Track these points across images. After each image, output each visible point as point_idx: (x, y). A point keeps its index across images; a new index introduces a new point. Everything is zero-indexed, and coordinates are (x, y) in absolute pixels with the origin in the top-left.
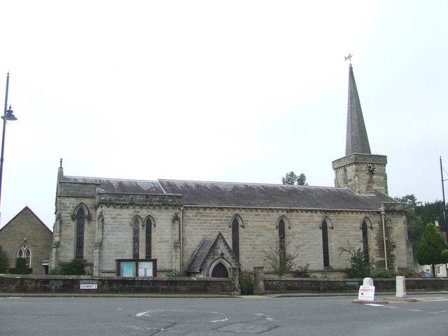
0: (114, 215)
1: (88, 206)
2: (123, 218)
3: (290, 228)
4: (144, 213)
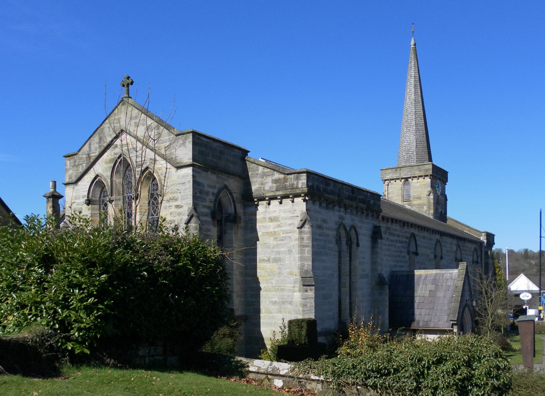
0: (319, 222)
1: (235, 195)
2: (328, 229)
3: (442, 258)
4: (349, 220)
